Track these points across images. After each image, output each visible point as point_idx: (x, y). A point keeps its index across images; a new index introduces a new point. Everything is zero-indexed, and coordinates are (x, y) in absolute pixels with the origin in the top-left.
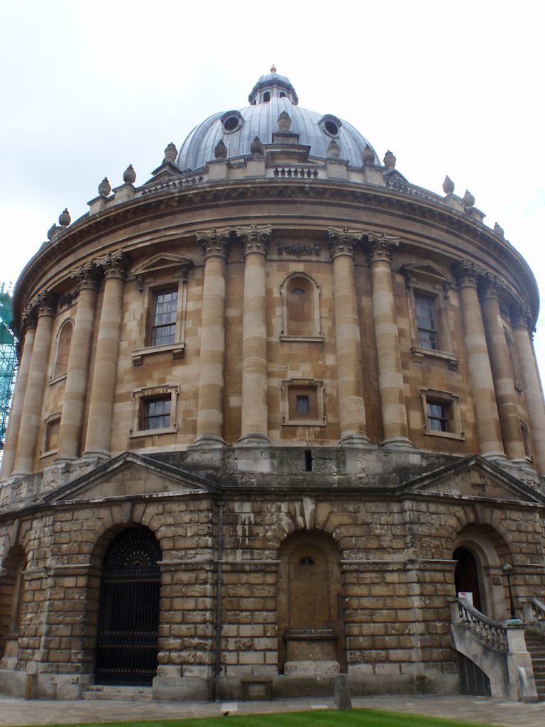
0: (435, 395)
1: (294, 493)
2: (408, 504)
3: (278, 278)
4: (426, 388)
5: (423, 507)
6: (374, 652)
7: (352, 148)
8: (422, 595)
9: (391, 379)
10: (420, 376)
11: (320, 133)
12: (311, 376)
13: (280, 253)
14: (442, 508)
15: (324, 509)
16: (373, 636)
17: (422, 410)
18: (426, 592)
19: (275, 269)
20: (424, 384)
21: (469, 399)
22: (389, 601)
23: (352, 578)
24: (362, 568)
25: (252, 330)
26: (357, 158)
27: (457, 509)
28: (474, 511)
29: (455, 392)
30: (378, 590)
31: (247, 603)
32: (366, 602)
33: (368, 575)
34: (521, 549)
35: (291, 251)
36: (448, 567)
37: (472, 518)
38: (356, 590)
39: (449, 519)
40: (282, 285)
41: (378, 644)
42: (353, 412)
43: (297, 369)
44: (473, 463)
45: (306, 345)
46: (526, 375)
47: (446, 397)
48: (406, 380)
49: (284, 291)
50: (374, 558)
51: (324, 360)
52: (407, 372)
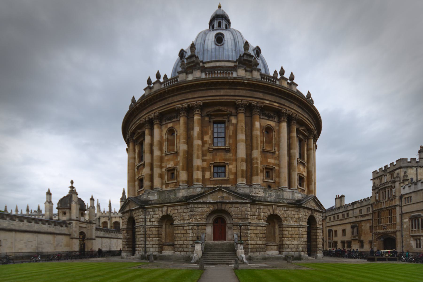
0: (217, 164)
1: (161, 204)
2: (191, 205)
3: (165, 130)
4: (213, 162)
5: (196, 206)
6: (180, 249)
7: (230, 47)
8: (192, 233)
9: (197, 162)
10: (211, 158)
11: (214, 46)
12: (173, 166)
13: (165, 121)
14: (205, 206)
15: (170, 209)
16: (180, 244)
17: (210, 171)
18: (194, 232)
19: (164, 128)
20: (213, 161)
21: (234, 163)
22: (185, 235)
23: (176, 228)
24: (178, 225)
25: (157, 153)
26: (232, 52)
27: (210, 205)
28: (217, 206)
29: (228, 161)
30: (182, 232)
31: (151, 236)
32: (179, 235)
33: (180, 228)
34: (237, 217)
35: (169, 119)
36: (204, 224)
37: (216, 208)
38: (177, 232)
39: (206, 209)
40: (166, 134)
41: (182, 247)
42: (183, 176)
43: (170, 164)
44: (218, 189)
45: (172, 155)
46: (281, 144)
47: (222, 164)
48: (203, 161)
49: (166, 136)
50: (182, 222)
51: (177, 159)
52: (205, 158)
